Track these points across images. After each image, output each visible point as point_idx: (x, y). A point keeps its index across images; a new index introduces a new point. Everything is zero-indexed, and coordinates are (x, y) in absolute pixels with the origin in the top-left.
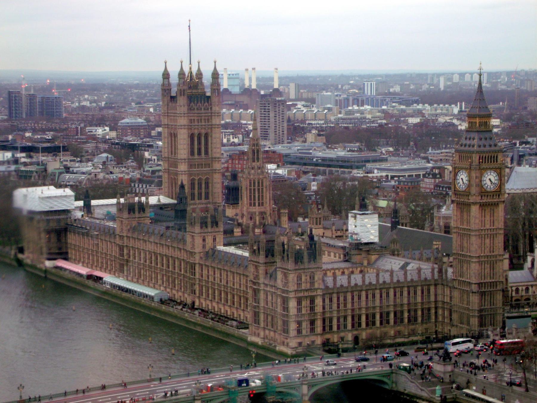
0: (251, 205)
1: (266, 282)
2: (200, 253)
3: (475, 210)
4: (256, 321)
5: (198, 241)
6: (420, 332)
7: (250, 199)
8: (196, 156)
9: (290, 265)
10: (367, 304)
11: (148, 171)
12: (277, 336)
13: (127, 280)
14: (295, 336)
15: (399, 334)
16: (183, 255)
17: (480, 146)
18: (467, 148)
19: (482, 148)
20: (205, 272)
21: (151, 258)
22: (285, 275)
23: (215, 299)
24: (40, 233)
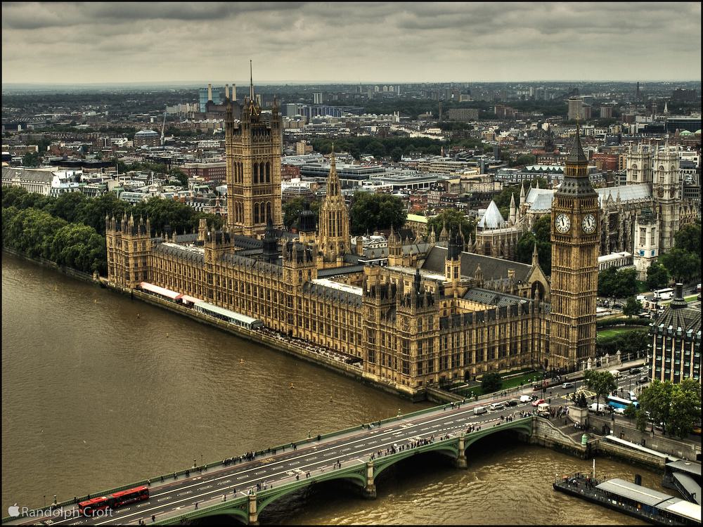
3: (575, 251)
4: (372, 360)
5: (295, 275)
7: (330, 230)
8: (259, 184)
9: (411, 311)
10: (477, 340)
11: (196, 190)
12: (395, 374)
13: (217, 305)
15: (502, 366)
16: (277, 287)
17: (579, 192)
18: (567, 193)
19: (582, 194)
20: (303, 304)
22: (406, 319)
23: (315, 330)
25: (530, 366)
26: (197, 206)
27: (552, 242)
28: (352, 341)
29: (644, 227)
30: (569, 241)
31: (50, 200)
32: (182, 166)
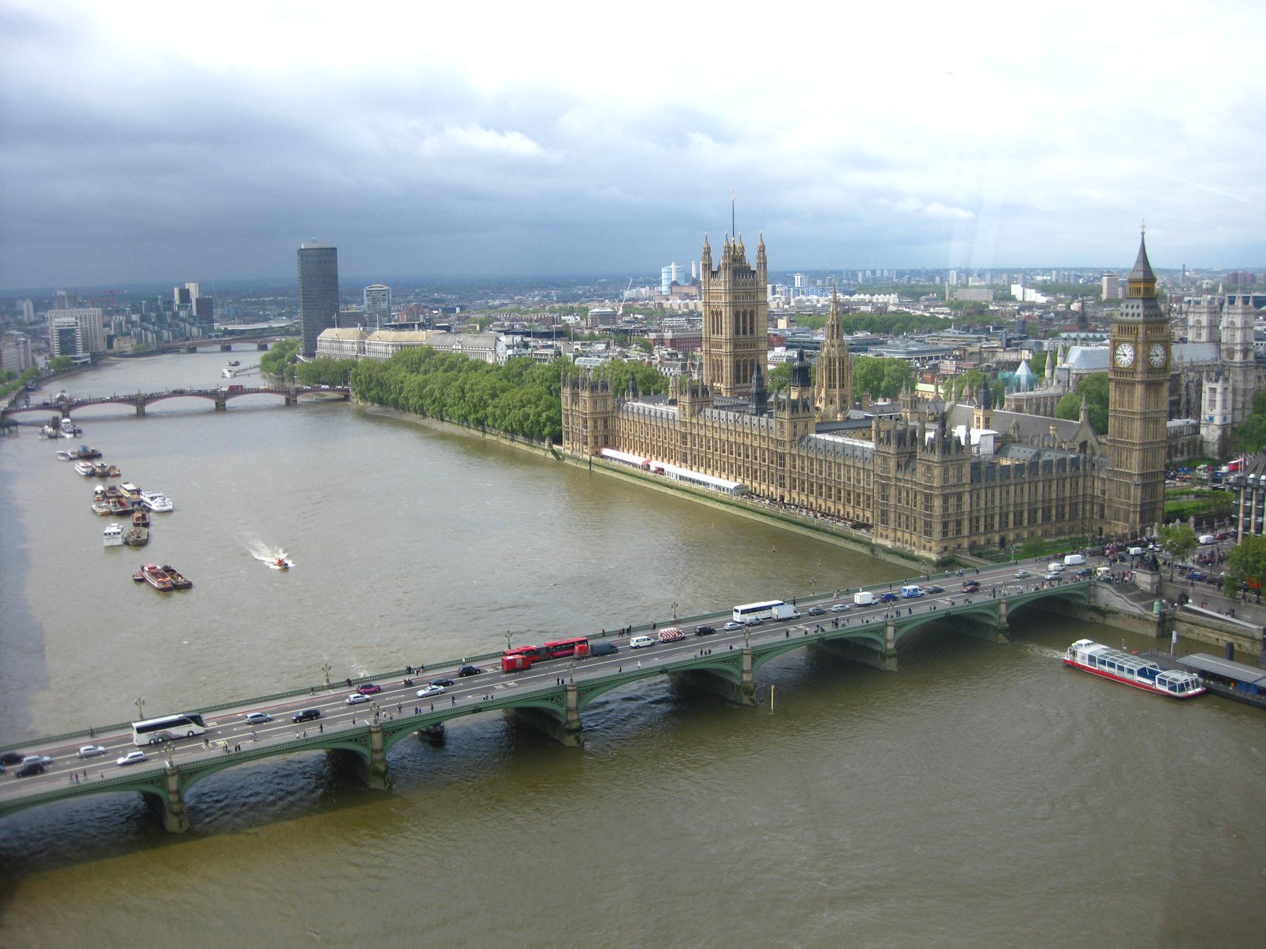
0: (830, 387)
1: (898, 476)
2: (791, 441)
3: (1139, 390)
6: (1067, 530)
8: (741, 335)
9: (936, 457)
10: (1015, 501)
12: (914, 538)
14: (942, 540)
15: (1046, 534)
17: (1145, 316)
18: (1130, 318)
21: (724, 446)
22: (929, 468)
24: (585, 421)
25: (1080, 536)
26: (665, 371)
27: (1110, 379)
28: (859, 503)
29: (1213, 385)
30: (1133, 377)
31: (496, 367)
32: (646, 337)
